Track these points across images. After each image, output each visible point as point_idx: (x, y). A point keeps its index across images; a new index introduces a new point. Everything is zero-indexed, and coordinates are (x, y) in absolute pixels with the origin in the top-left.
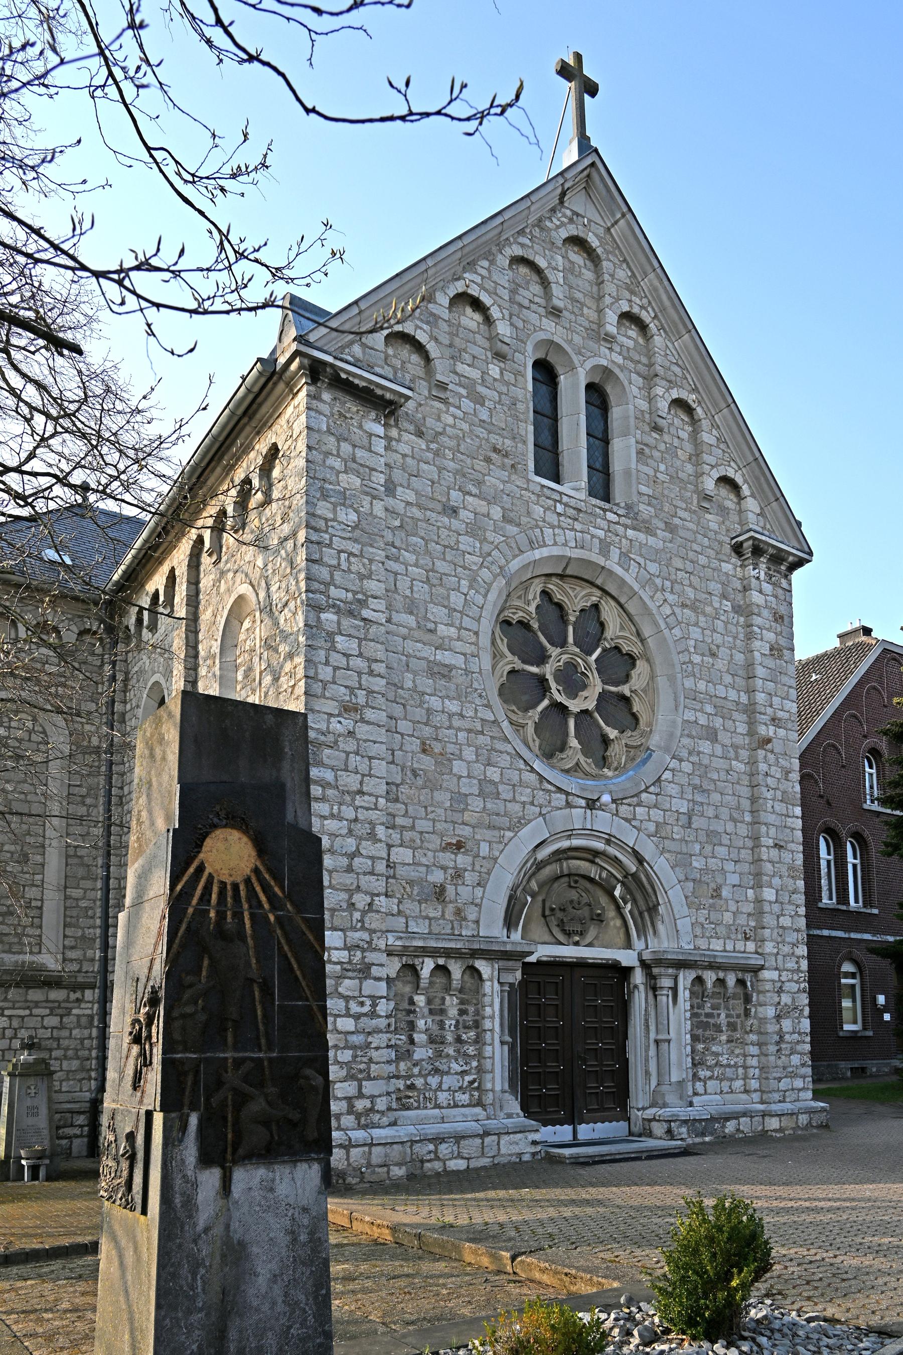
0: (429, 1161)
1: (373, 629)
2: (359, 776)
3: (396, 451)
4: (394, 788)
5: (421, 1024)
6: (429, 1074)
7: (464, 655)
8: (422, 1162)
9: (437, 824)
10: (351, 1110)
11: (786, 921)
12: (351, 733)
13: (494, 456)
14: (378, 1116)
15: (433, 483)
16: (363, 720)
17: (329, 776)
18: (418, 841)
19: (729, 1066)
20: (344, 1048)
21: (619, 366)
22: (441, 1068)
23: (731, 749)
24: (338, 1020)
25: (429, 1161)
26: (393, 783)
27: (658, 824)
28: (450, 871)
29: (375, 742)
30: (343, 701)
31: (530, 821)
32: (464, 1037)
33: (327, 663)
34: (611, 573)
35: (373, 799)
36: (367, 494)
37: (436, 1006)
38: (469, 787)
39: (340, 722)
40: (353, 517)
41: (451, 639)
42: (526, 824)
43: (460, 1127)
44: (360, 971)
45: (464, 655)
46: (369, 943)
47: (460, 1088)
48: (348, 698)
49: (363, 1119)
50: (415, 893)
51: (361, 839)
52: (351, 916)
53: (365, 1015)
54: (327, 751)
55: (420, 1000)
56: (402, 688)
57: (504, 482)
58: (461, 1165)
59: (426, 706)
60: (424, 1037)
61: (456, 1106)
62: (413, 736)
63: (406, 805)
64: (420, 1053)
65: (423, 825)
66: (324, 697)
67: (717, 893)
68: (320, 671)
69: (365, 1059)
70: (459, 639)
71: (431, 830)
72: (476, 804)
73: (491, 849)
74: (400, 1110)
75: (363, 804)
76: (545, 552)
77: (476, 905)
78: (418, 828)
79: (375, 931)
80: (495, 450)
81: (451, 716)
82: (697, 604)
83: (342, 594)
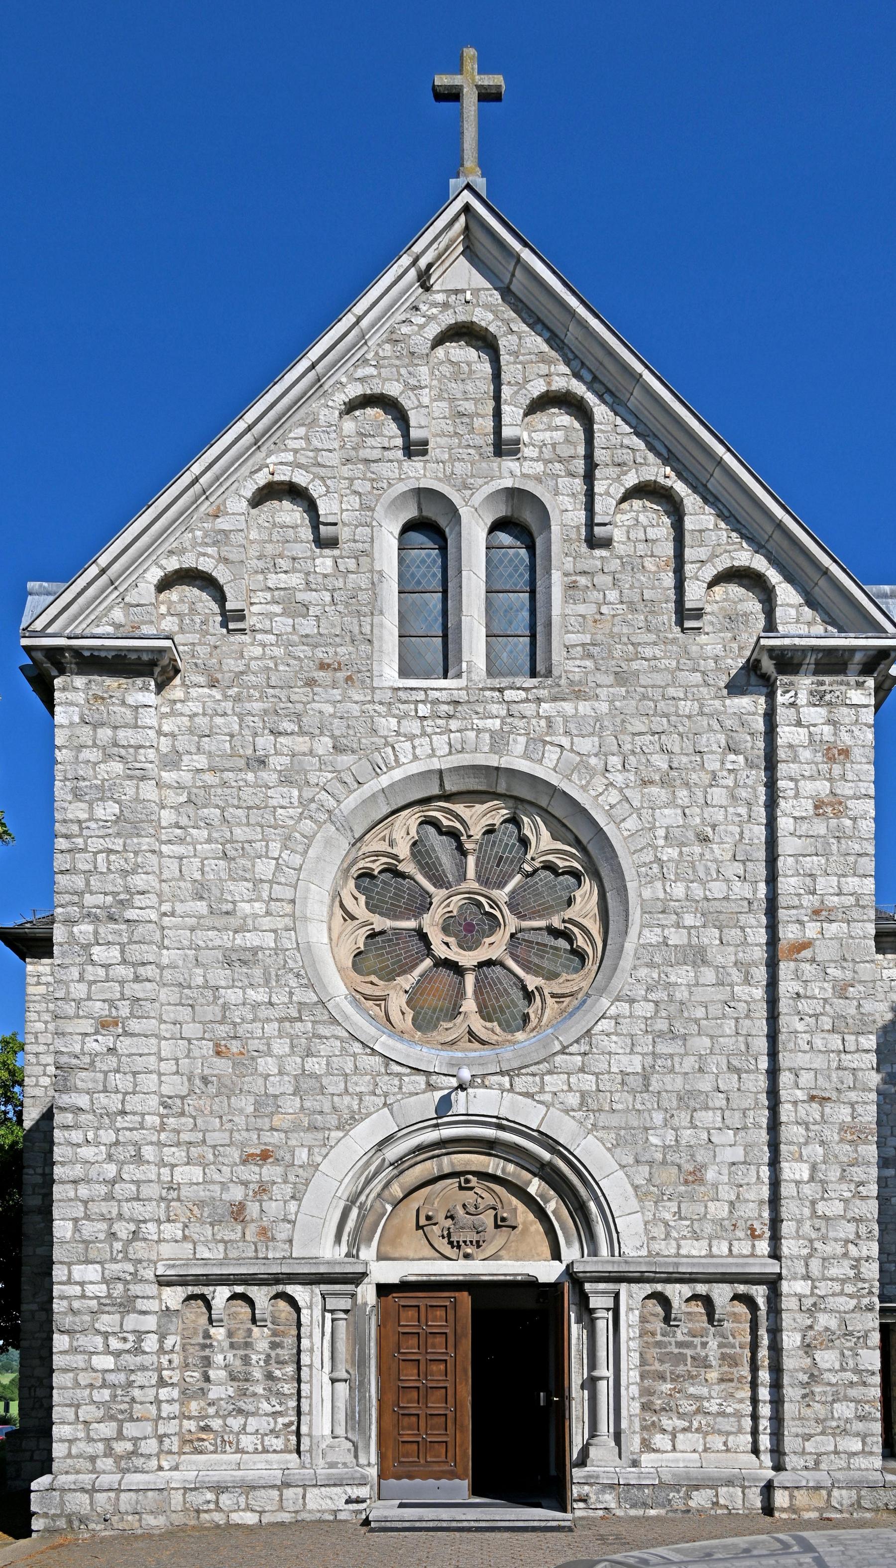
0: (206, 1511)
1: (140, 929)
2: (120, 1096)
3: (182, 714)
4: (178, 1102)
5: (219, 1359)
6: (229, 1414)
7: (275, 931)
8: (198, 1511)
9: (235, 1134)
10: (109, 1452)
11: (835, 1208)
12: (111, 1050)
13: (320, 675)
14: (142, 1460)
15: (232, 736)
16: (126, 1033)
17: (83, 1101)
18: (211, 1157)
19: (723, 1414)
20: (101, 1387)
21: (538, 479)
22: (244, 1407)
23: (734, 971)
24: (94, 1357)
25: (206, 1511)
26: (177, 1096)
27: (583, 1095)
28: (252, 1186)
29: (141, 1055)
30: (100, 1017)
31: (369, 1115)
32: (278, 1373)
33: (81, 979)
34: (512, 773)
35: (138, 1118)
36: (130, 778)
37: (239, 1338)
38: (281, 1086)
39: (97, 1041)
40: (116, 809)
41: (255, 916)
42: (363, 1119)
43: (250, 1475)
44: (121, 1305)
45: (275, 931)
46: (134, 1274)
47: (272, 1431)
48: (107, 1013)
49: (123, 1462)
50: (205, 1215)
51: (123, 1163)
52: (111, 1246)
53: (128, 1351)
54: (83, 1074)
55: (219, 1333)
56: (190, 987)
57: (334, 703)
58: (250, 1519)
59: (221, 1001)
60: (223, 1374)
61: (265, 1451)
62: (203, 1039)
63: (194, 1118)
64: (215, 1392)
65: (214, 1138)
66: (78, 1017)
67: (696, 1176)
68: (72, 990)
69: (127, 1399)
70: (268, 913)
71: (228, 1141)
72: (291, 1104)
73: (310, 1154)
74: (192, 1453)
75: (126, 1125)
76: (397, 774)
77: (289, 1222)
78: (209, 1142)
79: (140, 1261)
80: (323, 666)
81: (256, 1005)
82: (674, 774)
83: (99, 899)
